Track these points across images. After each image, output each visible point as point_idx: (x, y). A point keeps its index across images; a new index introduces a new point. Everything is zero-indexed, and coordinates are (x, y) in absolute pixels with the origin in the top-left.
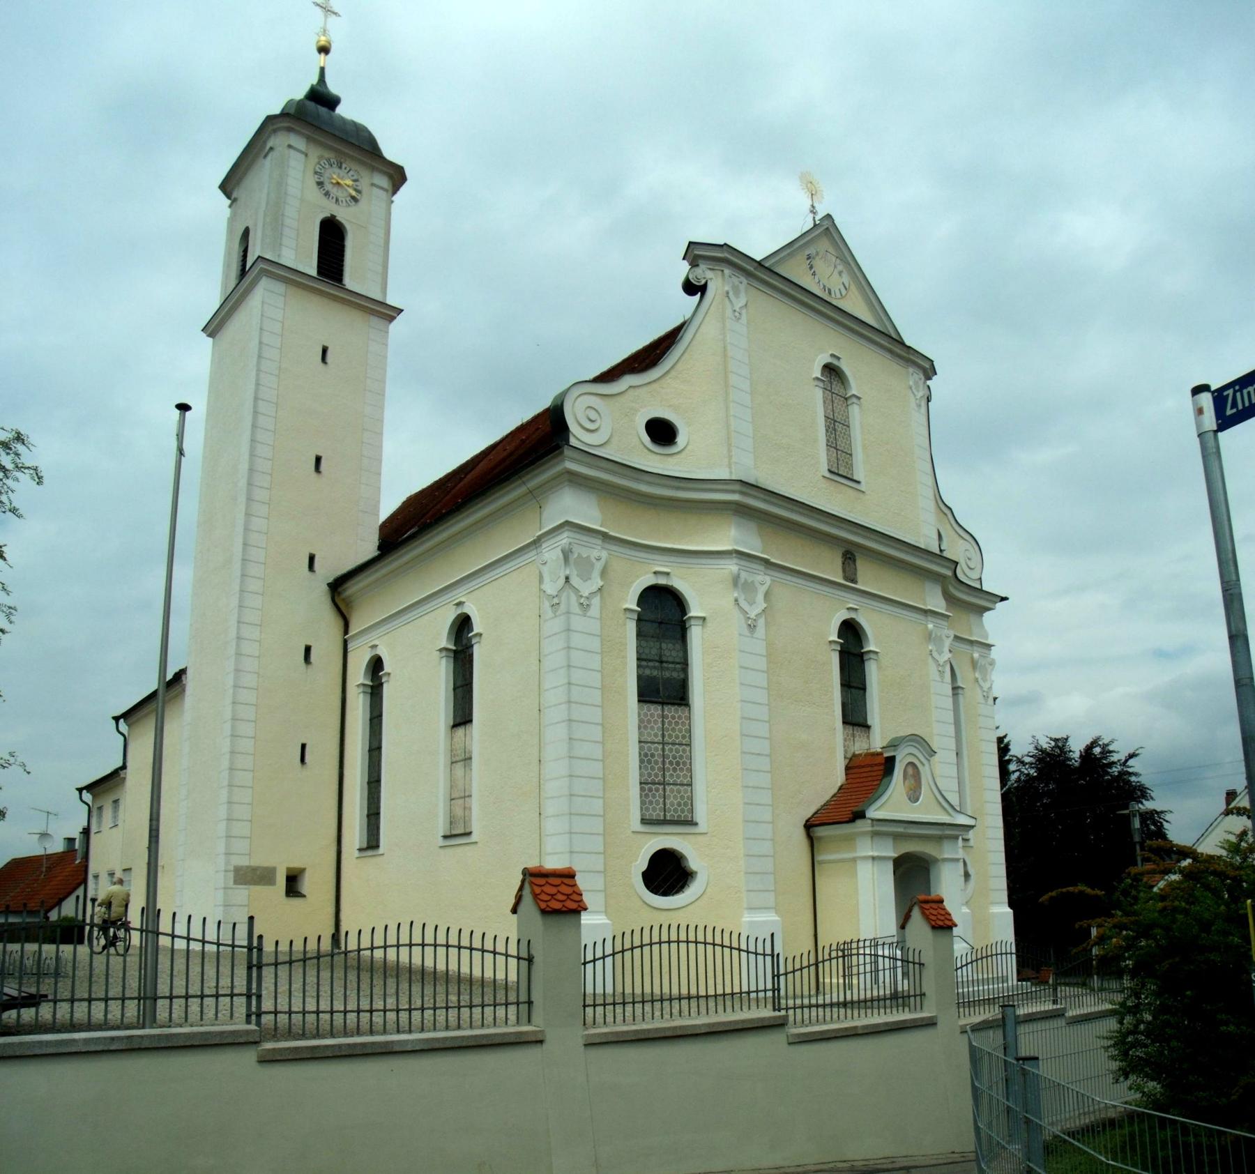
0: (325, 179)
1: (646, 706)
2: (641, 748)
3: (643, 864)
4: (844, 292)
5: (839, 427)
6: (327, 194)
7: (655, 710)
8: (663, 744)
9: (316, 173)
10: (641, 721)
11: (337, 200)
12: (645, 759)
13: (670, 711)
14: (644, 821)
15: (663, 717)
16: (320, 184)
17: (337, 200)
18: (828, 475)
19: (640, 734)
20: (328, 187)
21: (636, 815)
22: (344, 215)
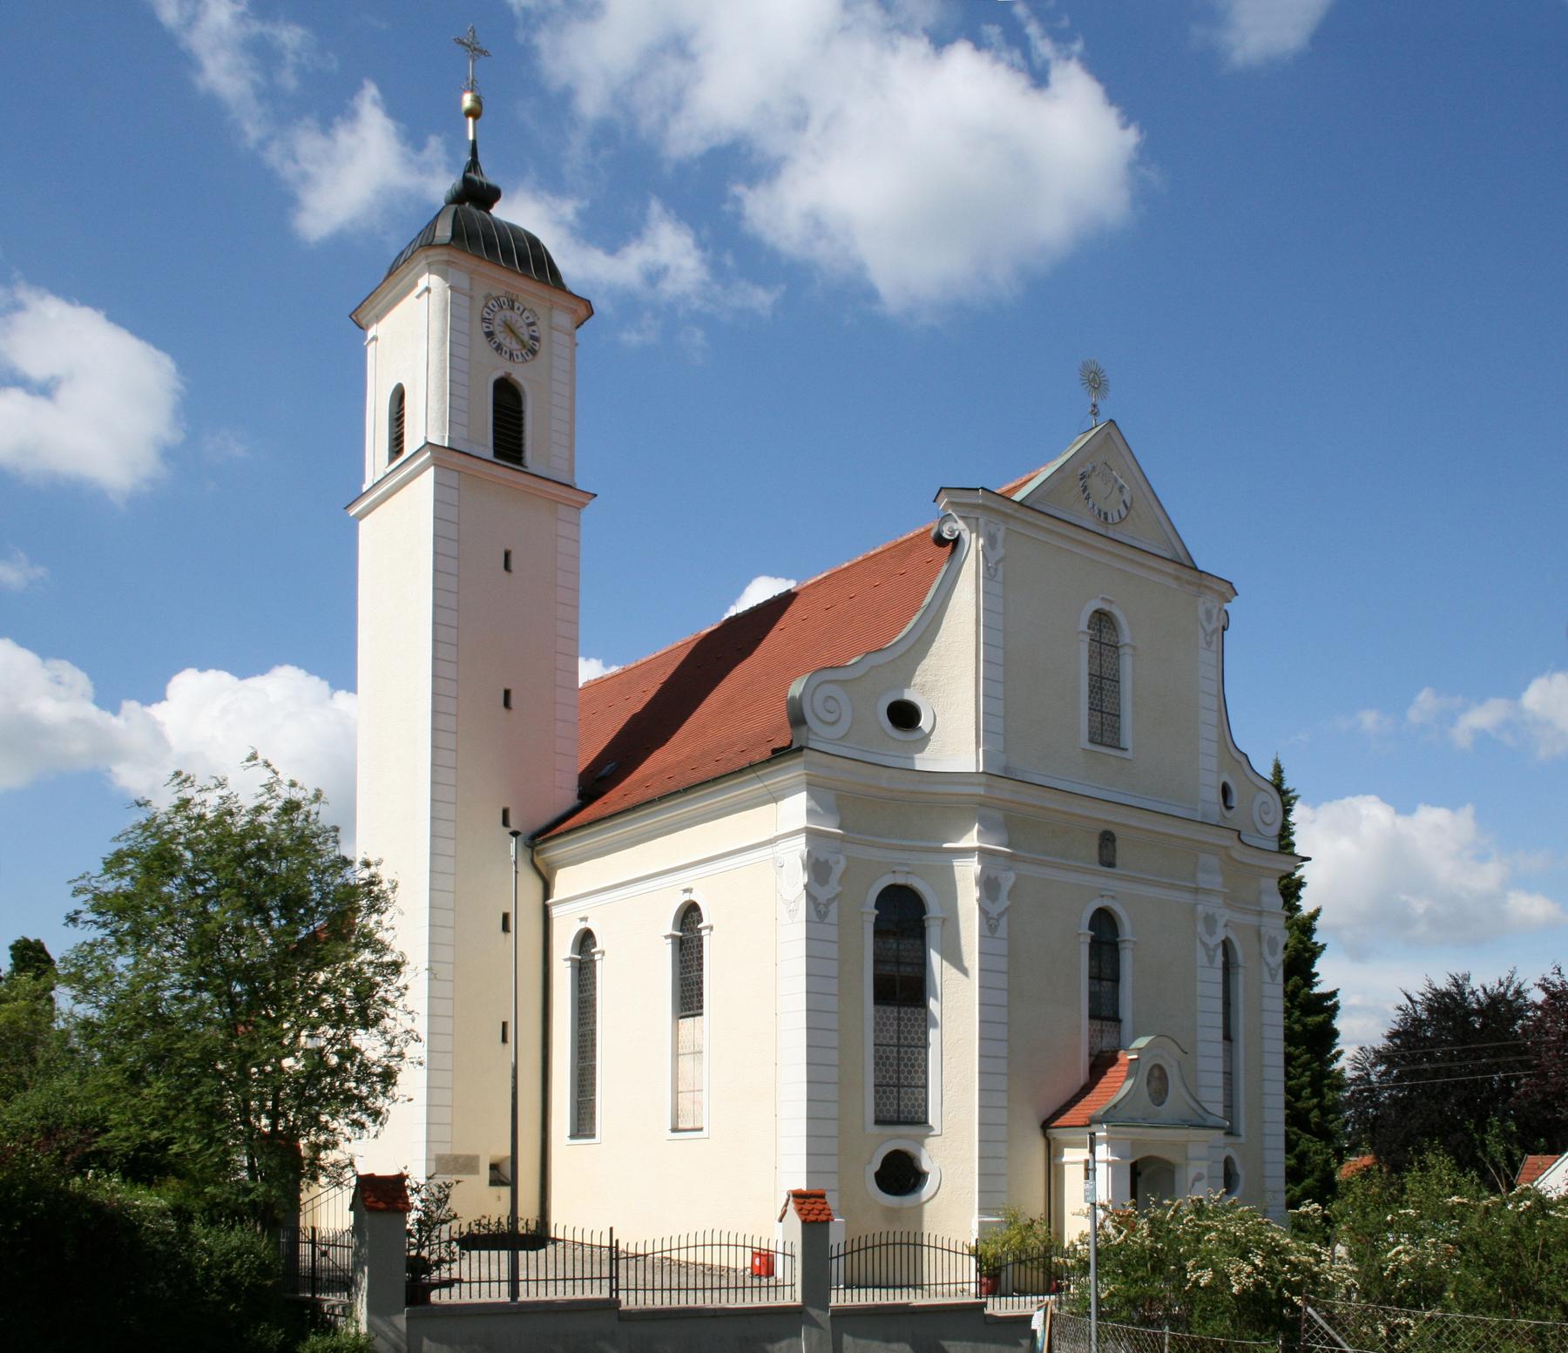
0: (498, 328)
1: (882, 1008)
2: (876, 1051)
3: (876, 1166)
4: (1124, 512)
5: (1107, 685)
6: (499, 348)
7: (891, 1012)
8: (899, 1046)
9: (484, 320)
10: (877, 1024)
12: (880, 1062)
13: (907, 1012)
14: (878, 1122)
15: (899, 1019)
16: (490, 335)
18: (1089, 746)
19: (876, 1037)
20: (501, 337)
21: (870, 1115)
22: (520, 374)
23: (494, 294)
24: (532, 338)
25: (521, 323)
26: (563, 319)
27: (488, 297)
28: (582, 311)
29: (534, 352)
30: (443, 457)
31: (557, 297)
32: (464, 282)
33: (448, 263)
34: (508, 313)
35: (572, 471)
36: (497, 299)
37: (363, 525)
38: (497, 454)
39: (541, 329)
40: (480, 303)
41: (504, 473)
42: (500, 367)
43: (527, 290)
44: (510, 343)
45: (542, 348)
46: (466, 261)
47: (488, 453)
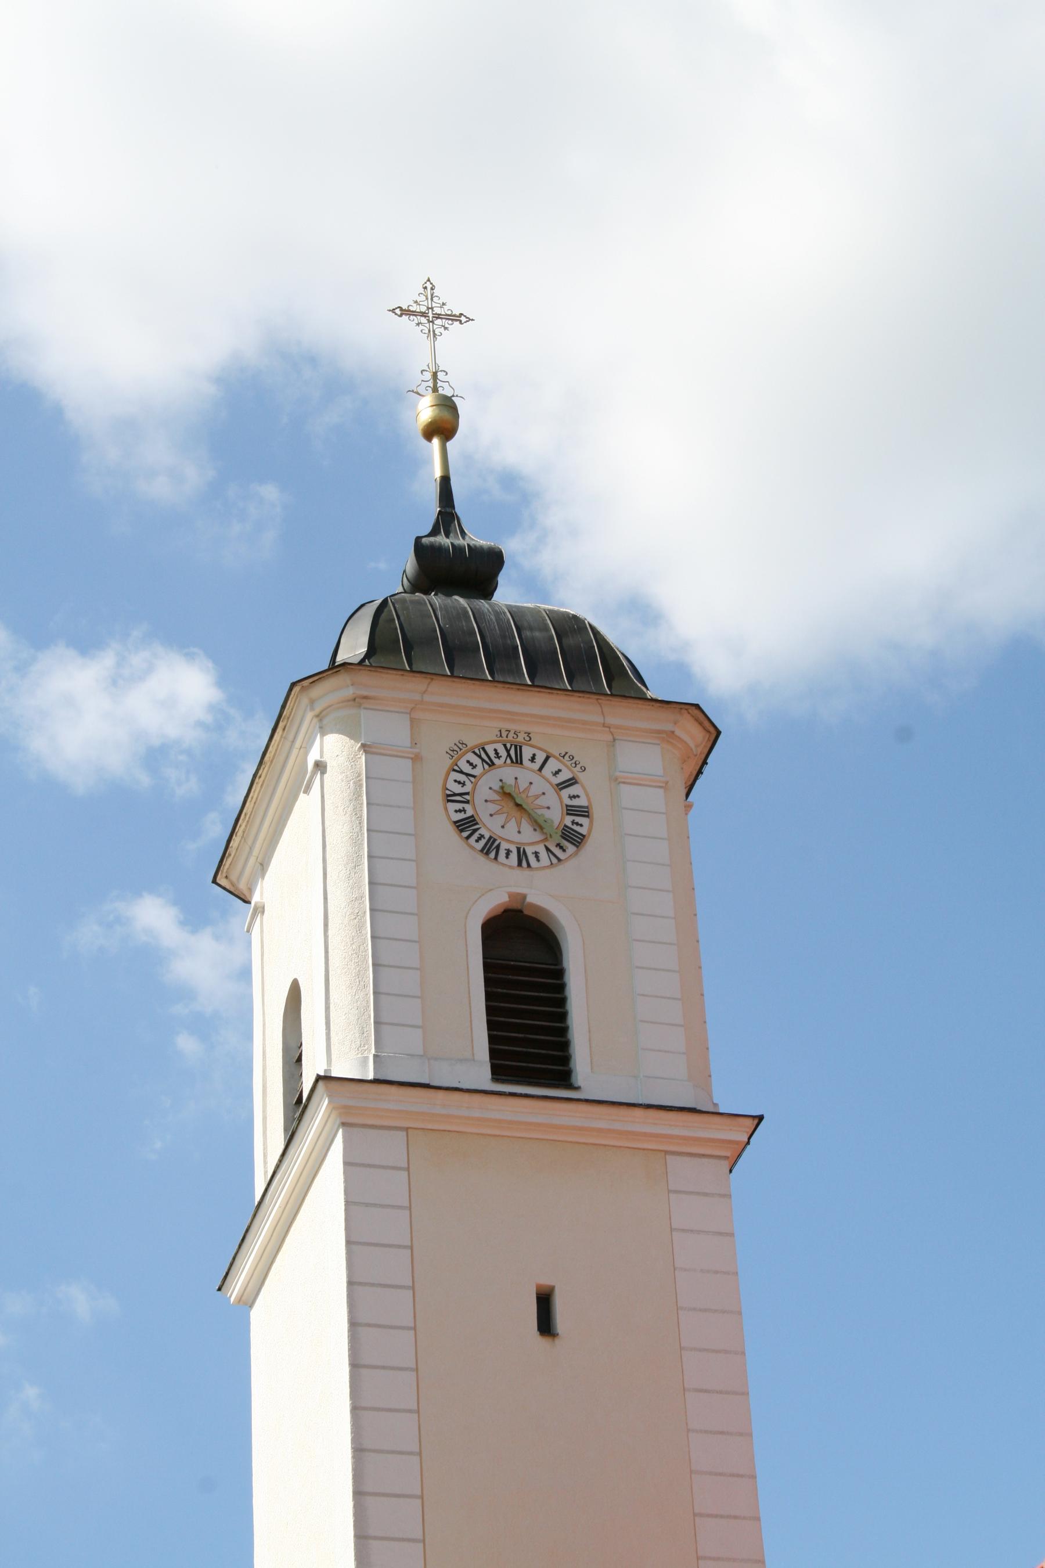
6: (491, 848)
9: (450, 798)
11: (522, 855)
16: (466, 826)
17: (522, 855)
20: (491, 825)
22: (545, 891)
23: (472, 741)
24: (571, 810)
25: (540, 785)
26: (645, 759)
27: (457, 750)
28: (692, 734)
29: (573, 838)
30: (373, 1104)
31: (621, 714)
32: (394, 729)
33: (358, 701)
34: (508, 773)
35: (702, 1077)
36: (480, 752)
37: (256, 1315)
38: (500, 1071)
39: (592, 789)
40: (438, 763)
41: (528, 1110)
42: (495, 888)
43: (549, 718)
44: (514, 833)
45: (599, 832)
46: (396, 687)
47: (481, 1075)
